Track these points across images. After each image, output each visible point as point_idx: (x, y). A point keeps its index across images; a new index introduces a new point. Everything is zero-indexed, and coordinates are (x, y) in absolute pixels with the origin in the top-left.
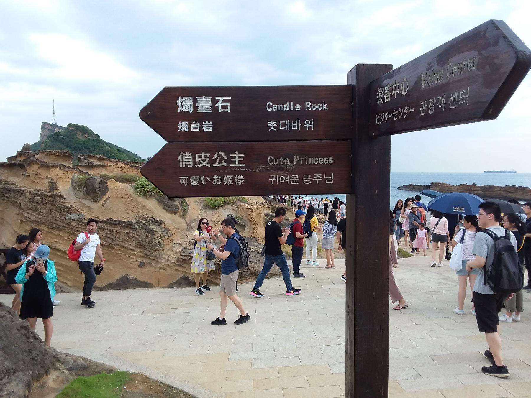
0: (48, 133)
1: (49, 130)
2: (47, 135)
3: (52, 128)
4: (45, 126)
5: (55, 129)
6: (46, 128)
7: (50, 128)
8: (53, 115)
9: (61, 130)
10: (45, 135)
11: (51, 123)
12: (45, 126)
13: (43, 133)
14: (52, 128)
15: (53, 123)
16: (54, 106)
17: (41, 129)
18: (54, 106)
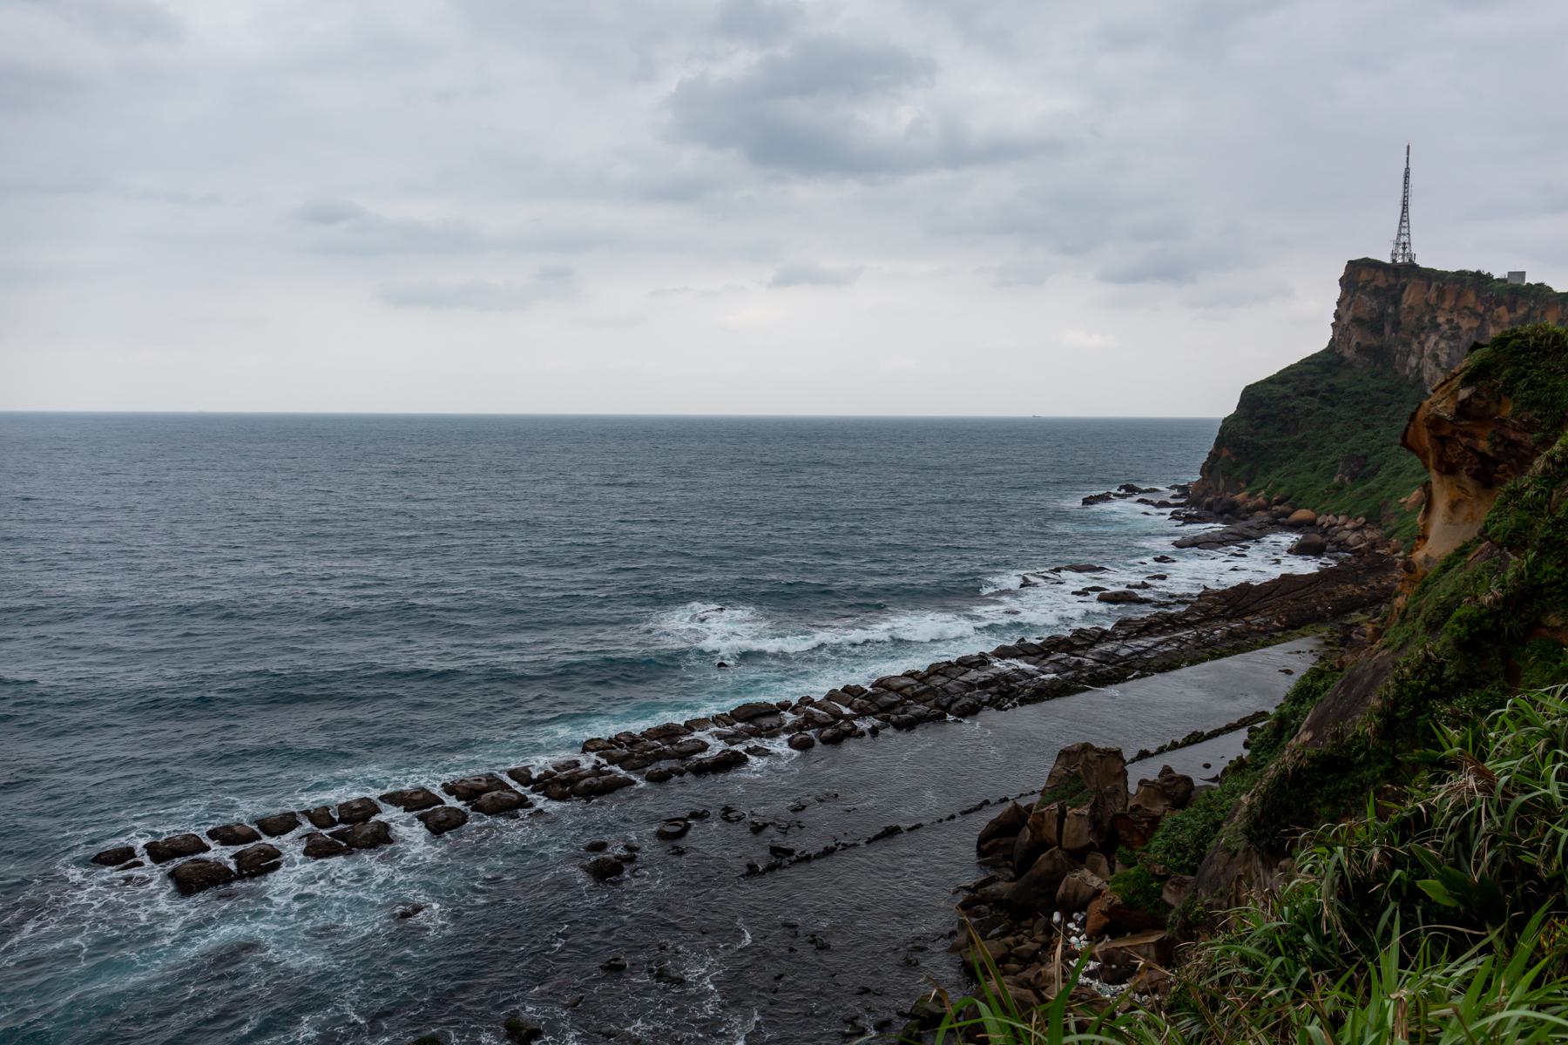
0: (1368, 305)
1: (1376, 292)
2: (1367, 318)
3: (1392, 281)
4: (1359, 276)
5: (1404, 287)
6: (1360, 284)
7: (1381, 282)
8: (1402, 221)
9: (1438, 287)
10: (1357, 320)
11: (1388, 261)
12: (1359, 276)
13: (1348, 309)
14: (1392, 281)
15: (1399, 261)
16: (1407, 176)
17: (1337, 292)
18: (1407, 176)
